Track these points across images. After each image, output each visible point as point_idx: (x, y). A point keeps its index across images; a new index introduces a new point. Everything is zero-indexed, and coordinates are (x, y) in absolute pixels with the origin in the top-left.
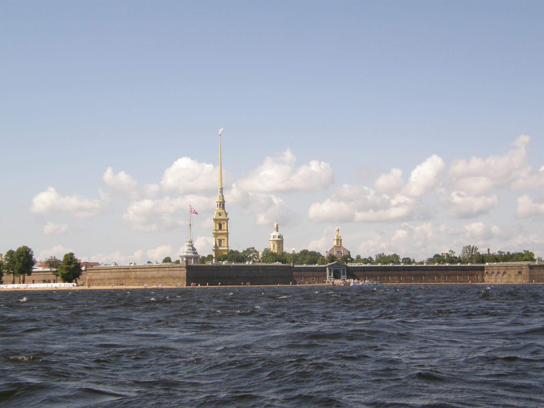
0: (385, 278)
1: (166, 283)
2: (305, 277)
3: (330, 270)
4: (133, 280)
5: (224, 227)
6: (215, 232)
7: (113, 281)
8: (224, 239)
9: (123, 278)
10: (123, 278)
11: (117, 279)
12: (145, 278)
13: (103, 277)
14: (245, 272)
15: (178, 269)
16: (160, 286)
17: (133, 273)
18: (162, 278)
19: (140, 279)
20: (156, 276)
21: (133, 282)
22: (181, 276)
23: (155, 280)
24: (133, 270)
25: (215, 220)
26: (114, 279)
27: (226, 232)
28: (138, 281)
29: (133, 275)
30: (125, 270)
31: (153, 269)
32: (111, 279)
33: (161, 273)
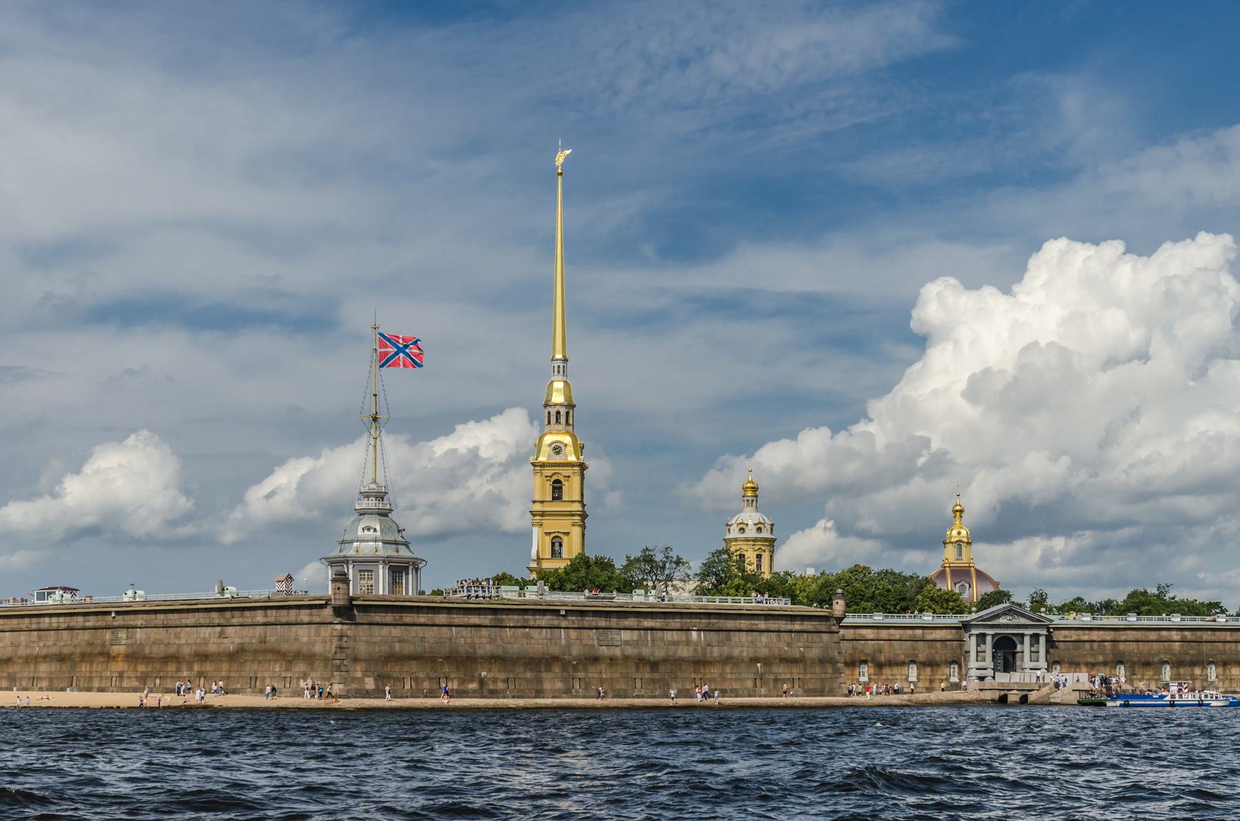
0: (1197, 671)
2: (879, 666)
3: (981, 638)
4: (120, 666)
5: (571, 490)
6: (538, 507)
7: (44, 668)
8: (568, 534)
9: (85, 657)
11: (61, 658)
12: (167, 659)
14: (625, 635)
16: (195, 698)
17: (122, 634)
18: (237, 656)
19: (147, 659)
20: (212, 648)
21: (121, 676)
22: (318, 648)
23: (208, 667)
24: (120, 621)
26: (46, 658)
27: (577, 507)
28: (141, 668)
29: (121, 643)
30: (92, 622)
31: (202, 618)
33: (235, 637)
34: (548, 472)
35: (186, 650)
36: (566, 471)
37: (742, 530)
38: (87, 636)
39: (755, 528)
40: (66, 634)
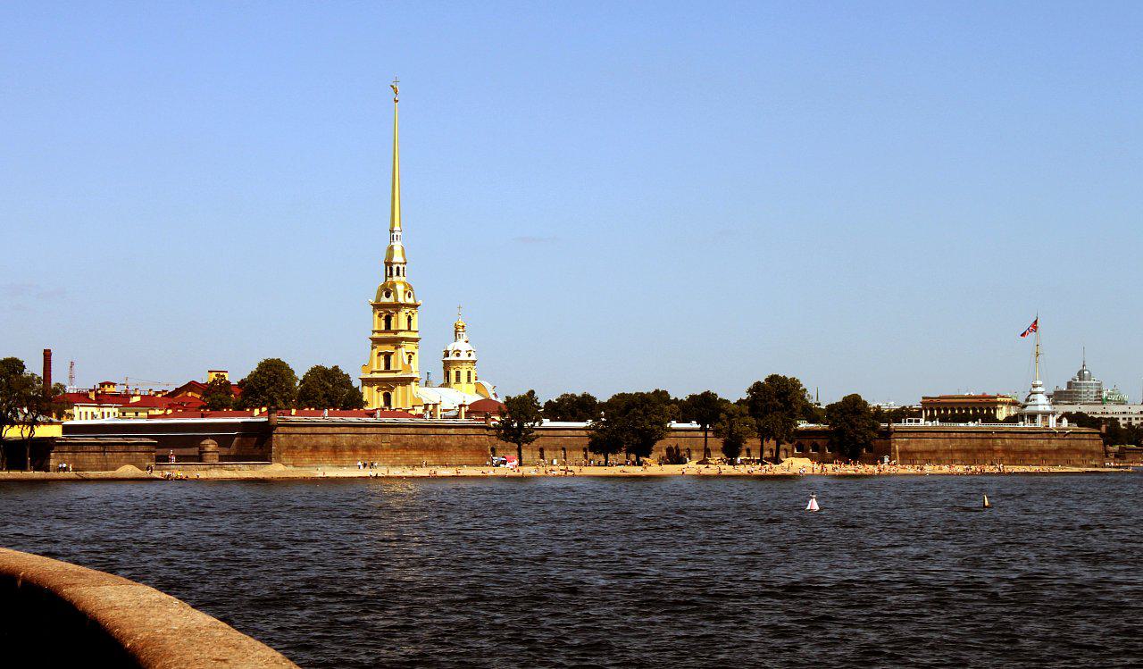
1: (1069, 463)
4: (1001, 455)
7: (957, 456)
8: (413, 353)
9: (979, 451)
10: (979, 451)
11: (967, 451)
13: (934, 447)
15: (1086, 436)
17: (999, 441)
18: (1059, 451)
19: (1015, 452)
20: (1047, 448)
22: (1094, 449)
23: (1046, 456)
24: (996, 436)
25: (377, 306)
26: (957, 451)
30: (980, 435)
32: (951, 451)
33: (1055, 444)
34: (407, 310)
35: (1033, 448)
36: (413, 311)
37: (458, 355)
38: (979, 441)
39: (467, 354)
40: (966, 441)
